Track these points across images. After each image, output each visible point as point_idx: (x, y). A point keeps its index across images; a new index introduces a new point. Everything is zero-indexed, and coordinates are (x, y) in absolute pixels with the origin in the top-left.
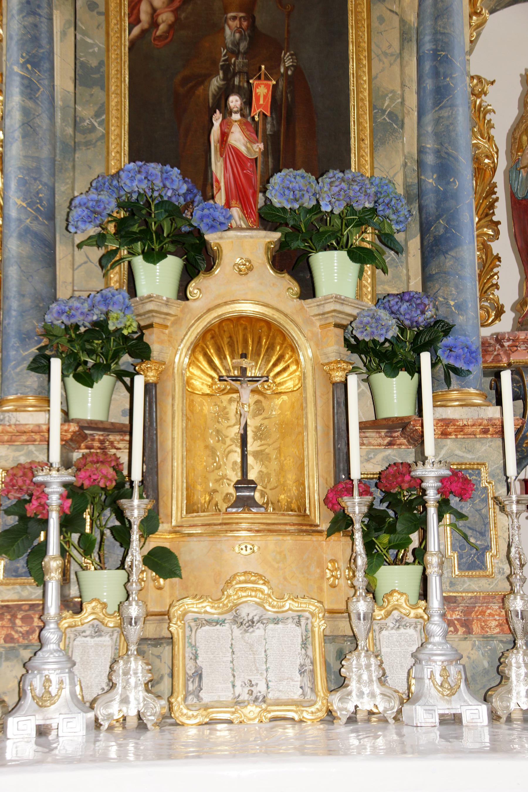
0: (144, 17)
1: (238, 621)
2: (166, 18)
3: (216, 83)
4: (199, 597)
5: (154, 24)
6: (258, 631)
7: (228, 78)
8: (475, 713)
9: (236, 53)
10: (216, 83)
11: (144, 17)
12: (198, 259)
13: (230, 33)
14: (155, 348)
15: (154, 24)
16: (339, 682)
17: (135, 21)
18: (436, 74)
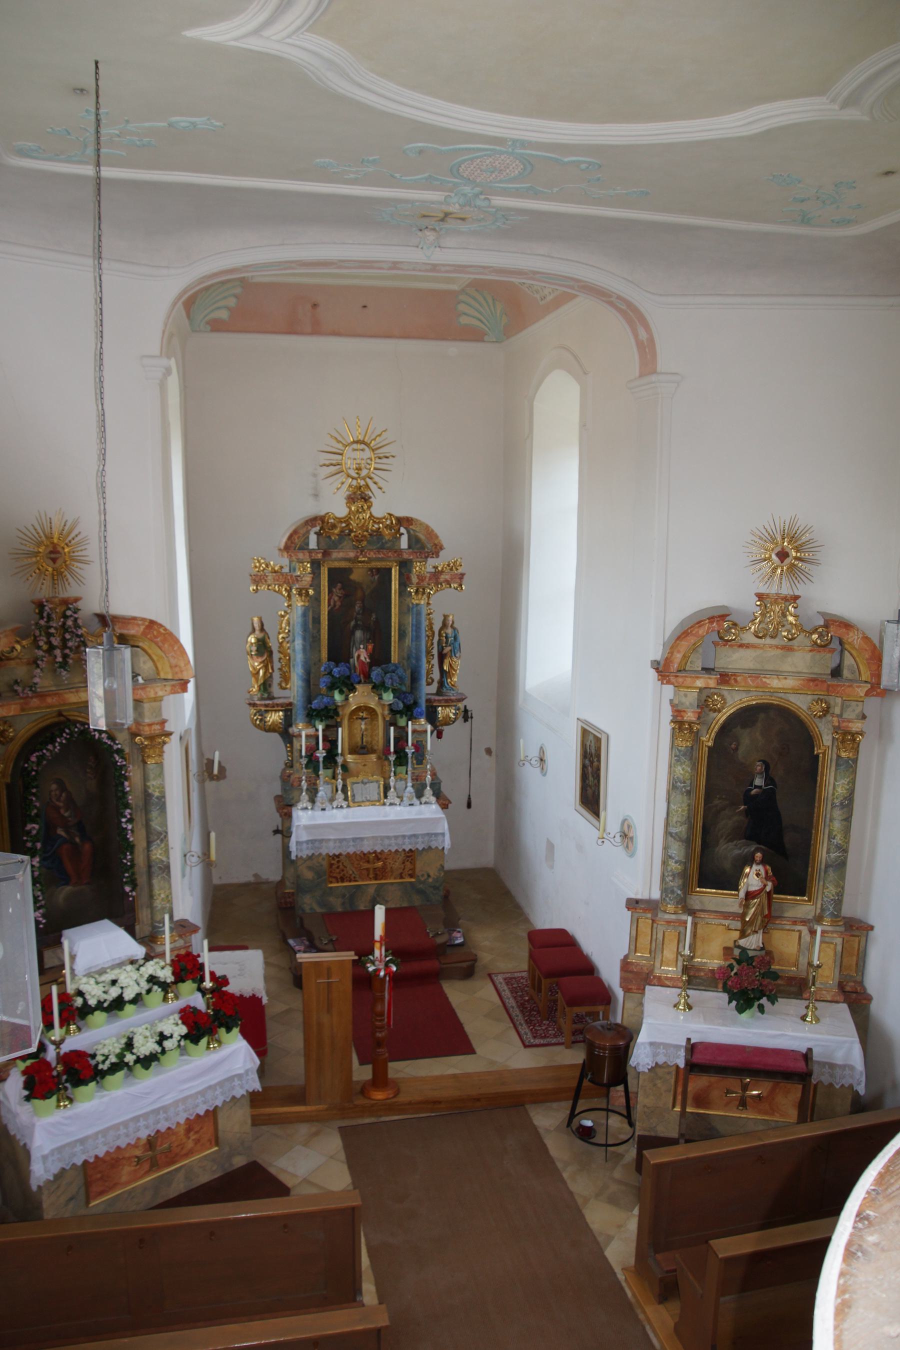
0: (332, 603)
1: (362, 782)
2: (338, 604)
3: (353, 623)
4: (352, 776)
5: (335, 606)
6: (367, 785)
7: (356, 621)
8: (416, 801)
9: (358, 614)
10: (353, 623)
11: (332, 603)
12: (352, 689)
13: (357, 608)
14: (341, 713)
15: (335, 606)
16: (386, 797)
17: (329, 604)
18: (416, 631)
